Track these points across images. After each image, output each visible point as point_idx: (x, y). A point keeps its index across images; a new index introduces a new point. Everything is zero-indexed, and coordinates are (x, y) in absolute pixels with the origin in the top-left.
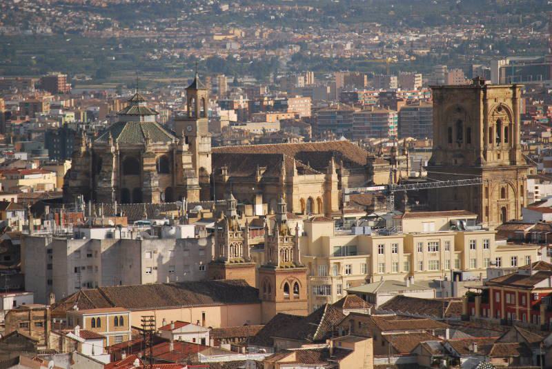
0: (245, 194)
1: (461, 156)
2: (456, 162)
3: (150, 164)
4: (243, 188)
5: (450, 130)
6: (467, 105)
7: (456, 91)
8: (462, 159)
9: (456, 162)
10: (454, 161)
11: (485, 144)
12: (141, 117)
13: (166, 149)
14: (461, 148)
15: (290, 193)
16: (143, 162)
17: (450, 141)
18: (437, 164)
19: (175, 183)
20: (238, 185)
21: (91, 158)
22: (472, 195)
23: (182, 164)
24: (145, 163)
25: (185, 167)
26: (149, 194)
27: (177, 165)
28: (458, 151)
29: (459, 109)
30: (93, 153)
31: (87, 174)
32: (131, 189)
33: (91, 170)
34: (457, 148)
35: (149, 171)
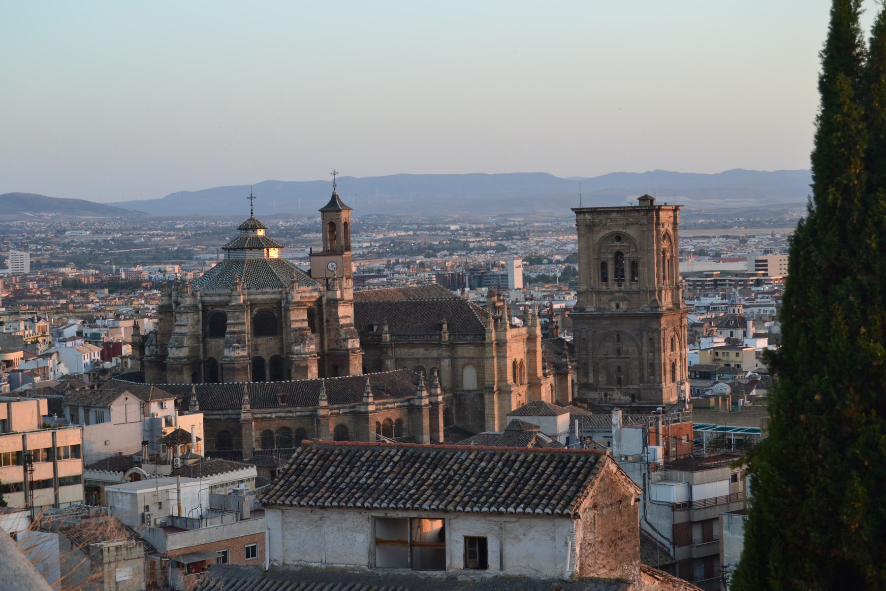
0: (418, 359)
1: (624, 299)
2: (618, 306)
3: (298, 318)
4: (415, 350)
5: (604, 265)
6: (631, 232)
7: (614, 215)
8: (625, 303)
9: (618, 306)
10: (613, 305)
11: (659, 282)
12: (265, 250)
13: (312, 297)
14: (623, 287)
15: (502, 357)
16: (287, 317)
17: (605, 279)
18: (587, 310)
19: (326, 348)
20: (404, 346)
21: (201, 313)
22: (645, 349)
23: (337, 319)
24: (292, 318)
25: (342, 322)
26: (303, 364)
27: (327, 321)
28: (618, 292)
29: (619, 238)
30: (203, 306)
31: (194, 336)
32: (267, 358)
33: (201, 332)
34: (616, 288)
35: (301, 329)
